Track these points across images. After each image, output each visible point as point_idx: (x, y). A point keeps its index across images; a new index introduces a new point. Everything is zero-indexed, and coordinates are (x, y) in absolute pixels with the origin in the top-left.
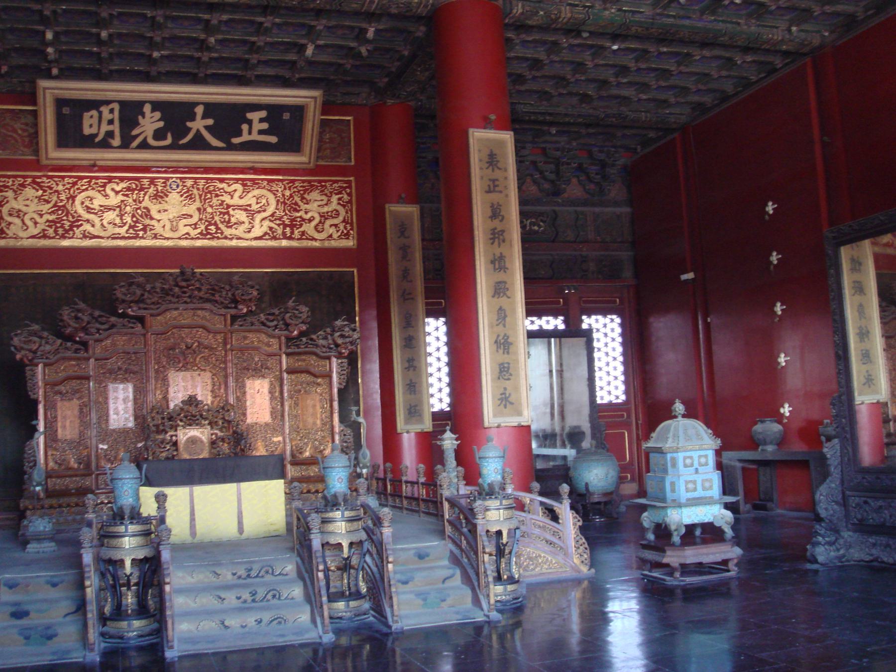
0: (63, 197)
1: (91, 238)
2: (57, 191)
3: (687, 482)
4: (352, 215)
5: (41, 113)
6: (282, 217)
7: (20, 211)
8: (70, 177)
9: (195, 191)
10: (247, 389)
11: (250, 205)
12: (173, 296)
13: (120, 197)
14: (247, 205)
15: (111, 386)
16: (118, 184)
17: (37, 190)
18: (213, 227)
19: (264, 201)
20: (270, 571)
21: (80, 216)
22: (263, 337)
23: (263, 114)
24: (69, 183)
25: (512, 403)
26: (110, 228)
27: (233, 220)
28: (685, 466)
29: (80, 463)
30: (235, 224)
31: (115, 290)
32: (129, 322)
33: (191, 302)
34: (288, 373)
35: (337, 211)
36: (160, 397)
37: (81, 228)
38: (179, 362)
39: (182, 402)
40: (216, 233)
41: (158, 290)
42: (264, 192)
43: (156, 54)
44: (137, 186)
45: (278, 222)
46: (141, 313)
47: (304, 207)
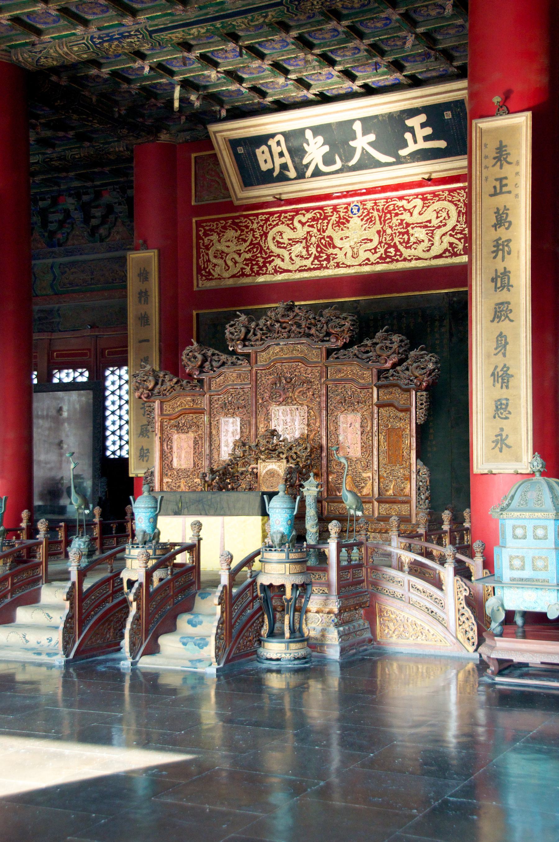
0: (257, 235)
1: (281, 273)
3: (511, 558)
5: (219, 156)
6: (464, 230)
7: (223, 252)
8: (263, 214)
9: (375, 213)
10: (340, 423)
11: (430, 221)
14: (427, 222)
15: (223, 420)
16: (304, 215)
17: (236, 231)
18: (392, 250)
19: (444, 214)
21: (272, 252)
22: (356, 369)
23: (422, 118)
24: (262, 220)
25: (509, 447)
26: (298, 261)
27: (412, 239)
28: (515, 537)
30: (414, 243)
32: (239, 359)
33: (289, 337)
34: (379, 406)
36: (263, 430)
37: (273, 264)
42: (446, 203)
45: (459, 236)
46: (246, 350)
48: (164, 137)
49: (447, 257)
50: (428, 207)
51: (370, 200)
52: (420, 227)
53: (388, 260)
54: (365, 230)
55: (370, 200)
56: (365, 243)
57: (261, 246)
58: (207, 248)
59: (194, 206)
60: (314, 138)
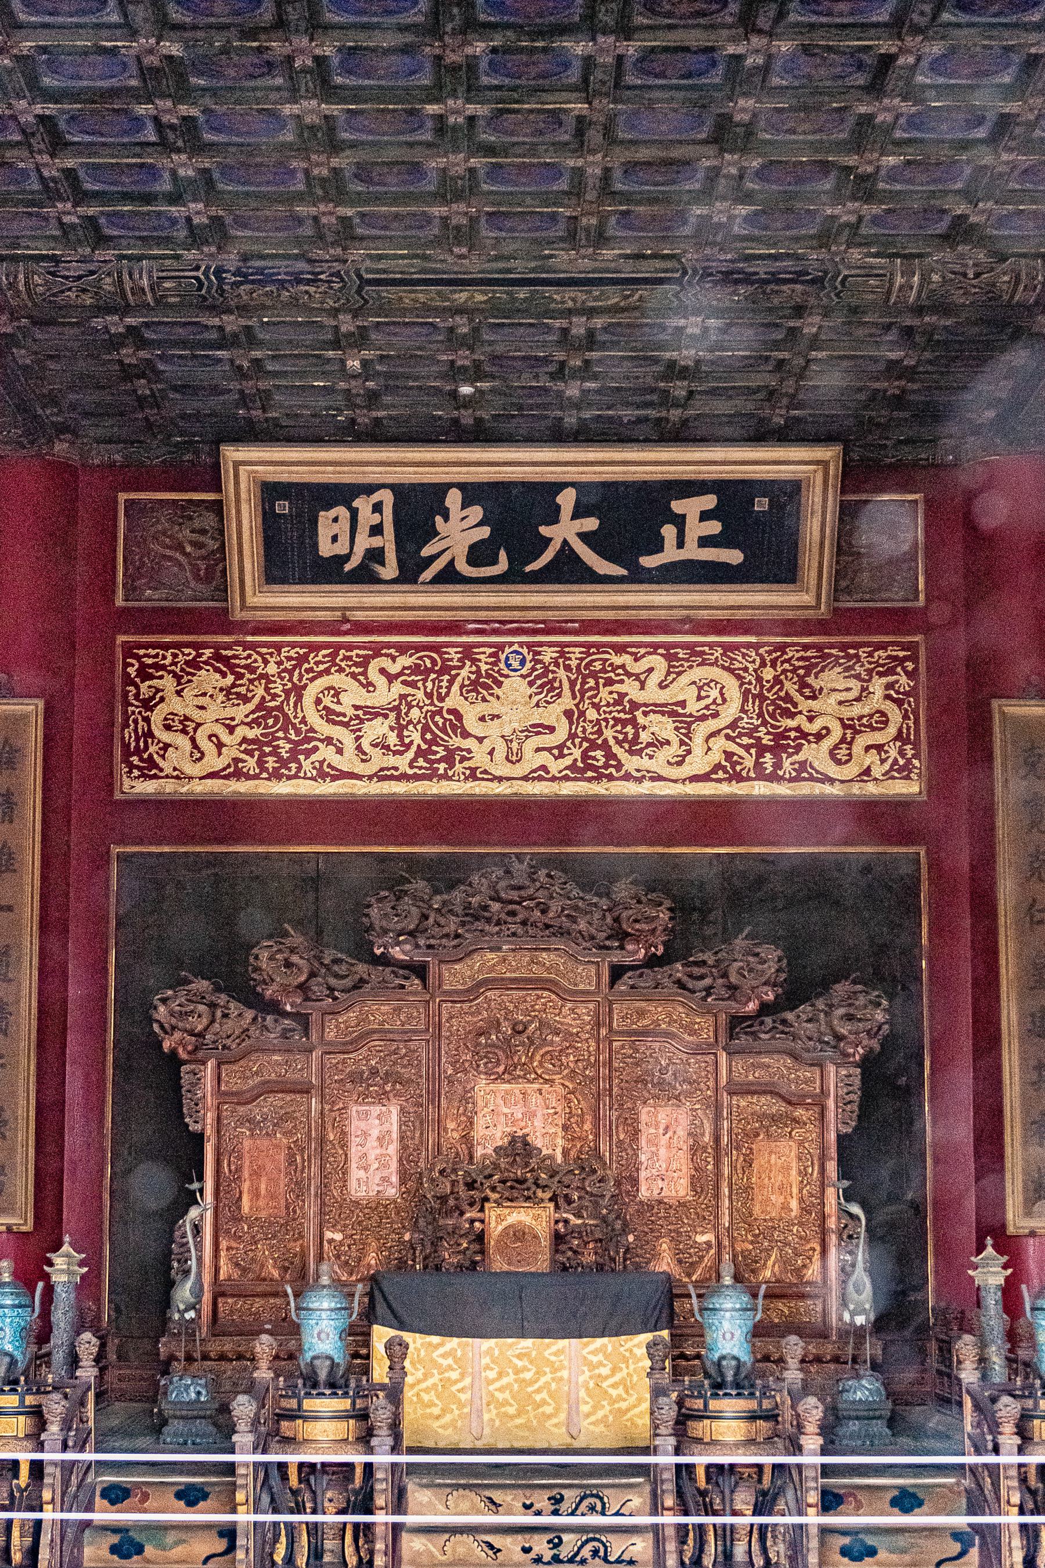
0: (278, 689)
1: (334, 778)
2: (265, 676)
4: (916, 722)
6: (756, 729)
7: (187, 718)
8: (293, 645)
9: (562, 673)
11: (683, 704)
12: (488, 920)
13: (398, 688)
14: (676, 704)
15: (354, 1109)
16: (394, 659)
18: (599, 754)
19: (714, 693)
20: (599, 1508)
21: (312, 730)
23: (709, 501)
24: (289, 658)
26: (376, 753)
27: (645, 737)
29: (286, 1269)
30: (649, 745)
31: (369, 906)
34: (731, 1094)
35: (883, 714)
36: (456, 1135)
37: (314, 757)
38: (498, 1063)
39: (497, 1150)
40: (606, 766)
41: (459, 910)
42: (715, 672)
43: (466, 390)
44: (434, 662)
45: (746, 741)
47: (804, 705)
48: (60, 447)
49: (719, 781)
50: (679, 674)
51: (551, 644)
52: (663, 713)
53: (590, 774)
54: (537, 705)
55: (551, 644)
56: (538, 733)
57: (286, 716)
58: (148, 705)
59: (125, 609)
60: (464, 507)
